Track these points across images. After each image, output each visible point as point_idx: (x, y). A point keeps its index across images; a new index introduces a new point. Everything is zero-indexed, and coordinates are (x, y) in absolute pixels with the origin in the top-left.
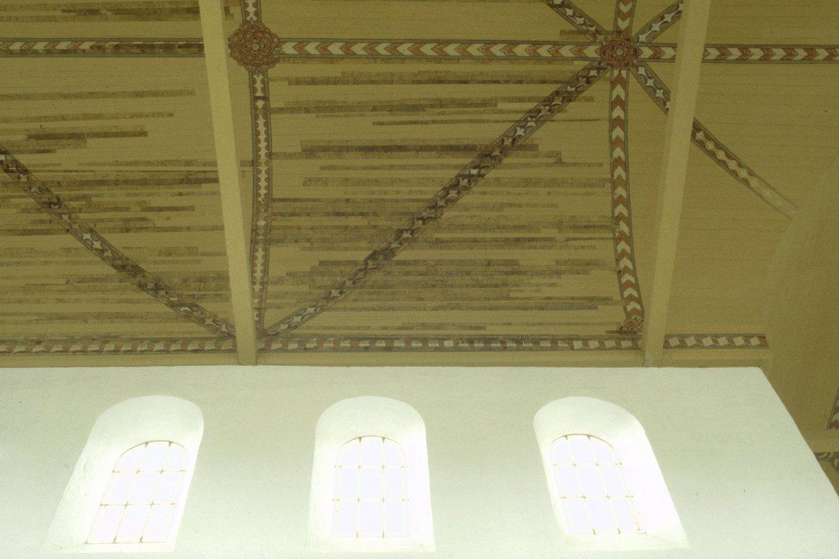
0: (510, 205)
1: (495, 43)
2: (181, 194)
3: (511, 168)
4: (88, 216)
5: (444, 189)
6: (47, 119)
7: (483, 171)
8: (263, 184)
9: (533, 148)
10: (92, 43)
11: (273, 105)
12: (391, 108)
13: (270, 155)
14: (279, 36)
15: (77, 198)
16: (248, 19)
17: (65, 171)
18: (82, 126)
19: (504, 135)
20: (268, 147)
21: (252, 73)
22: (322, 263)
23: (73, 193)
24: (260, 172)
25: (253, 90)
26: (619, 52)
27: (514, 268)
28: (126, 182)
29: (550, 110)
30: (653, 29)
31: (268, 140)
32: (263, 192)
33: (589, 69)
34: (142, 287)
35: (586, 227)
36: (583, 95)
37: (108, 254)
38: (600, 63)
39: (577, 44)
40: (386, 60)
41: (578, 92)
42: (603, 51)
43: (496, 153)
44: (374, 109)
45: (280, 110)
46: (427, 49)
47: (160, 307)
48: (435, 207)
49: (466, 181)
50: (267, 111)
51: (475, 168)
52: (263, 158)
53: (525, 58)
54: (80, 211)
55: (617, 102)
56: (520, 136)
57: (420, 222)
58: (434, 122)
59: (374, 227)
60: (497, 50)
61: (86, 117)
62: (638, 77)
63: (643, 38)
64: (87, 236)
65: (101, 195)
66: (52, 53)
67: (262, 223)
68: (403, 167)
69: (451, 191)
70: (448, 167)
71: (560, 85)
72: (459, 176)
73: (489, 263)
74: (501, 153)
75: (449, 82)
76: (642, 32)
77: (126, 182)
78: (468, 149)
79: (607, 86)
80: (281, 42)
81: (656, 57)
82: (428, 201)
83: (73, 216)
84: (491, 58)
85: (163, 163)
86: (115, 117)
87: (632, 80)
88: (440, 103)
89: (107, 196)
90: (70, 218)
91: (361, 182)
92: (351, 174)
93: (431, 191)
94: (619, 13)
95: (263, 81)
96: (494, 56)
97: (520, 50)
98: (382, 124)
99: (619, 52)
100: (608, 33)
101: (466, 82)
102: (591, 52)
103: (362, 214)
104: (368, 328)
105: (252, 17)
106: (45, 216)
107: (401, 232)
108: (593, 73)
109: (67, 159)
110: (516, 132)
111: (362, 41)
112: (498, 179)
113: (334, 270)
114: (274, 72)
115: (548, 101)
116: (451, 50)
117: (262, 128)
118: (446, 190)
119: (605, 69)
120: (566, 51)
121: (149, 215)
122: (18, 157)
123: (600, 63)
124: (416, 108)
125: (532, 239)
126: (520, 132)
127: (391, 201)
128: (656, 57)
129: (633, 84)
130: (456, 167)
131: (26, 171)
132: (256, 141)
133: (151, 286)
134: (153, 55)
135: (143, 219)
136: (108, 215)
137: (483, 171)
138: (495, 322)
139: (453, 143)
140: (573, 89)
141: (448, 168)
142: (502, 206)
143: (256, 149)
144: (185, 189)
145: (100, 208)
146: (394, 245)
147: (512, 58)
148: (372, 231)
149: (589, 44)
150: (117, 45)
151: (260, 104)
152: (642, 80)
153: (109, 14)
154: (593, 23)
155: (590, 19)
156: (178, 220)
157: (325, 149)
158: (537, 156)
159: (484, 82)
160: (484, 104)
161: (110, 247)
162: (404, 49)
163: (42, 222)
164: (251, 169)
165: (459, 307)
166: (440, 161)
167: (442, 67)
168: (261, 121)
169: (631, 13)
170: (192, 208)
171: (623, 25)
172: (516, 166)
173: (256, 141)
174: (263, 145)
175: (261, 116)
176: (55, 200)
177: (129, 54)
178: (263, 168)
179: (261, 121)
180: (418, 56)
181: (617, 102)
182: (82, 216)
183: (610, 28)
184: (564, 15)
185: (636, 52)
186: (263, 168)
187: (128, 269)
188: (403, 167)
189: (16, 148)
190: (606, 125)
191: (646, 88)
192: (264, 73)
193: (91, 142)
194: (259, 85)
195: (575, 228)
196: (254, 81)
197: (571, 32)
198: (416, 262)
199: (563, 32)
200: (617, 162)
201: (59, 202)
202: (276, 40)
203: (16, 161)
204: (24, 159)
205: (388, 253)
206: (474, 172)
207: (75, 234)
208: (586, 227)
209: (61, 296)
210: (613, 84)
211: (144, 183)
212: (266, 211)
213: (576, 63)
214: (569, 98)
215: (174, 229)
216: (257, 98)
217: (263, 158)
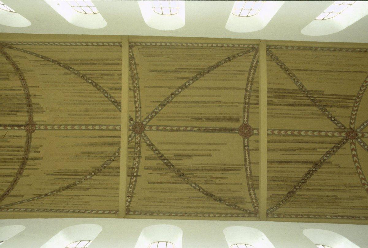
0: (328, 179)
1: (315, 131)
2: (223, 174)
4: (194, 179)
5: (305, 174)
6: (181, 150)
7: (316, 169)
8: (249, 171)
9: (330, 162)
10: (198, 128)
11: (250, 148)
12: (285, 150)
13: (250, 163)
14: (253, 128)
15: (189, 174)
16: (244, 122)
17: (185, 166)
18: (192, 153)
19: (321, 159)
20: (249, 160)
21: (244, 139)
22: (273, 195)
23: (188, 172)
24: (247, 168)
25: (244, 144)
26: (352, 135)
27: (336, 198)
28: (205, 170)
29: (333, 152)
30: (361, 128)
31: (249, 158)
32: (249, 174)
33: (343, 140)
34: (215, 200)
35: (355, 186)
36: (342, 147)
37: (201, 190)
38: (346, 138)
39: (339, 132)
40: (283, 135)
41: (341, 146)
42: (347, 134)
44: (281, 150)
45: (253, 150)
46: (296, 133)
47: (223, 206)
48: (304, 179)
49: (312, 172)
50: (249, 150)
51: (314, 168)
54: (191, 177)
55: (353, 150)
56: (325, 159)
57: (301, 184)
58: (299, 154)
59: (286, 185)
60: (316, 133)
61: (193, 150)
62: (358, 142)
63: (358, 130)
64: (194, 185)
65: (197, 173)
66: (185, 131)
68: (292, 168)
69: (308, 175)
70: (305, 168)
71: (335, 144)
72: (309, 170)
73: (327, 196)
74: (321, 164)
75: (303, 143)
76: (358, 128)
77: (205, 170)
78: (310, 163)
80: (253, 129)
81: (363, 136)
82: (301, 177)
83: (188, 179)
84: (314, 136)
85: (217, 164)
86: (201, 150)
87: (357, 143)
88: (300, 149)
89: (199, 173)
90: (187, 180)
91: (278, 172)
92: (276, 169)
93: (302, 175)
94: (351, 123)
95: (247, 141)
96: (315, 135)
97: (323, 134)
98: (283, 155)
99: (352, 135)
100: (347, 129)
101: (307, 143)
102: (343, 134)
103: (281, 181)
104: (298, 212)
105: (246, 122)
106: (179, 179)
108: (345, 141)
109: (186, 162)
110: (324, 158)
111: (277, 130)
112: (321, 172)
113: (278, 197)
114: (250, 138)
115: (332, 149)
116: (302, 133)
117: (247, 155)
118: (306, 174)
119: (348, 140)
120: (336, 134)
121: (214, 180)
122: (171, 161)
123: (346, 138)
124: (293, 150)
125: (339, 189)
126: (325, 158)
127: (290, 177)
128: (363, 136)
130: (308, 168)
131: (173, 165)
132: (245, 159)
133: (218, 200)
134: (215, 132)
135: (211, 181)
136: (200, 179)
137: (316, 169)
138: (340, 212)
140: (339, 145)
141: (305, 168)
142: (325, 180)
143: (246, 161)
145: (197, 177)
146: (294, 190)
147: (320, 136)
148: (286, 186)
149: (342, 132)
150: (205, 129)
151: (246, 148)
153: (204, 119)
154: (343, 126)
156: (222, 181)
158: (332, 165)
159: (313, 143)
160: (314, 149)
161: (202, 188)
162: (289, 133)
163: (178, 180)
164: (244, 167)
165: (323, 208)
166: (302, 166)
167: (300, 138)
168: (247, 153)
169: (354, 123)
170: (227, 178)
171: (352, 126)
172: (326, 168)
173: (245, 159)
174: (247, 160)
175: (246, 151)
176: (182, 174)
177: (207, 132)
178: (248, 167)
179: (247, 153)
180: (293, 135)
181: (353, 150)
182: (191, 179)
183: (348, 127)
184: (335, 123)
185: (357, 135)
186: (248, 167)
187: (209, 195)
188: (292, 168)
189: (170, 159)
190: (351, 157)
193: (194, 158)
194: (246, 142)
195: (351, 187)
196: (244, 141)
197: (337, 128)
198: (304, 195)
199: (334, 128)
200: (357, 168)
201: (183, 175)
202: (252, 129)
203: (170, 162)
204: (172, 162)
205: (293, 192)
206: (314, 169)
207: (190, 184)
208: (355, 186)
209: (188, 202)
210: (351, 144)
211: (210, 170)
212: (251, 179)
213: (339, 138)
214: (338, 148)
216: (245, 146)
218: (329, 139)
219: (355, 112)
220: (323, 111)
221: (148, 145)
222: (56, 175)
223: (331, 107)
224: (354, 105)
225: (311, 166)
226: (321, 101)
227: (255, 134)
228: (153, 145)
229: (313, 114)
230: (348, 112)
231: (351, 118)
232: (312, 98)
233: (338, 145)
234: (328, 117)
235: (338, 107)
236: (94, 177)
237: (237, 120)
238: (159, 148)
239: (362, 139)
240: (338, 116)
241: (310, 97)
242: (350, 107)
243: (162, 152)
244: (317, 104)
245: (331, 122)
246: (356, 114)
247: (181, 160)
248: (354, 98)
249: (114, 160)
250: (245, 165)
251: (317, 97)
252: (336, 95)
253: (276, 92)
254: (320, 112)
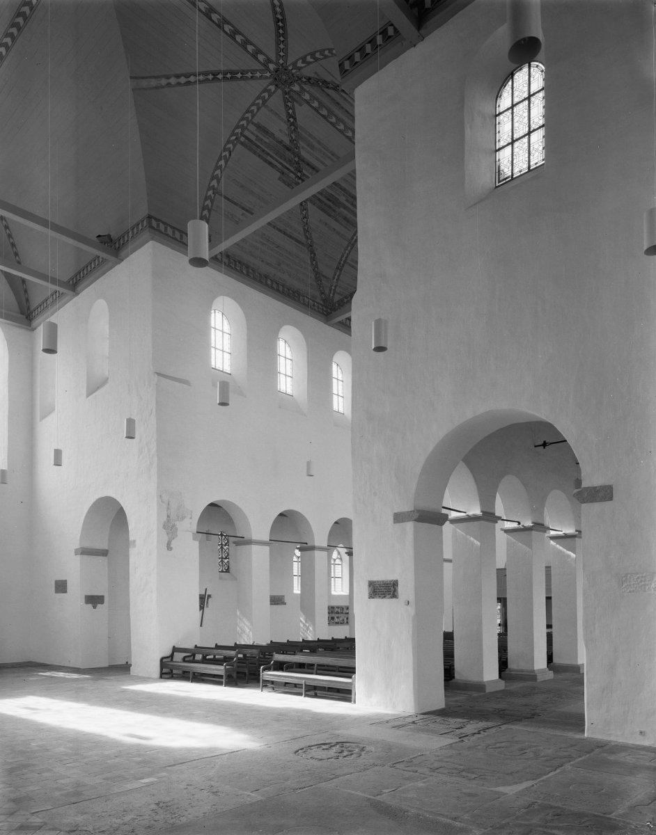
1: (331, 123)
33: (305, 83)
53: (325, 107)
60: (333, 120)
76: (266, 78)
79: (302, 71)
81: (269, 61)
97: (324, 112)
102: (296, 88)
108: (304, 80)
120: (307, 97)
128: (269, 61)
129: (290, 60)
147: (331, 112)
152: (285, 57)
154: (285, 99)
155: (285, 101)
169: (265, 90)
171: (272, 88)
183: (279, 91)
184: (294, 112)
185: (277, 71)
191: (286, 54)
197: (297, 102)
214: (325, 82)
218: (325, 101)
219: (252, 108)
220: (295, 142)
223: (281, 142)
224: (248, 124)
226: (290, 162)
229: (312, 147)
230: (262, 117)
231: (265, 101)
232: (299, 174)
233: (321, 84)
234: (297, 128)
235: (272, 135)
239: (274, 59)
240: (282, 120)
241: (300, 178)
242: (255, 125)
244: (297, 159)
245: (298, 117)
246: (253, 104)
248: (242, 139)
251: (292, 172)
252: (266, 161)
253: (334, 211)
254: (301, 143)
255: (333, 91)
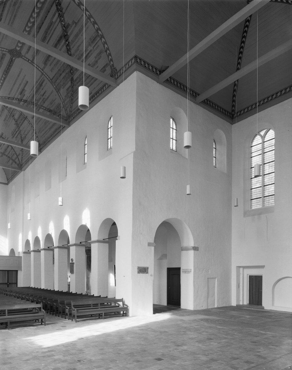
2: (42, 89)
3: (72, 32)
13: (42, 70)
21: (21, 58)
25: (26, 60)
29: (61, 11)
32: (49, 79)
43: (66, 34)
52: (42, 72)
56: (64, 24)
58: (50, 37)
61: (20, 84)
67: (55, 87)
71: (55, 3)
78: (61, 38)
101: (43, 23)
107: (70, 71)
115: (58, 9)
135: (44, 98)
139: (58, 39)
144: (42, 88)
157: (46, 61)
158: (71, 27)
160: (51, 24)
186: (44, 74)
192: (22, 56)
193: (25, 89)
206: (67, 43)
215: (48, 97)
217: (42, 72)
221: (9, 99)
222: (14, 136)
225: (64, 41)
227: (20, 49)
228: (9, 97)
233: (57, 2)
236: (21, 128)
237: (4, 55)
238: (13, 96)
243: (16, 97)
247: (24, 95)
249: (14, 115)
250: (43, 74)
255: (56, 8)
